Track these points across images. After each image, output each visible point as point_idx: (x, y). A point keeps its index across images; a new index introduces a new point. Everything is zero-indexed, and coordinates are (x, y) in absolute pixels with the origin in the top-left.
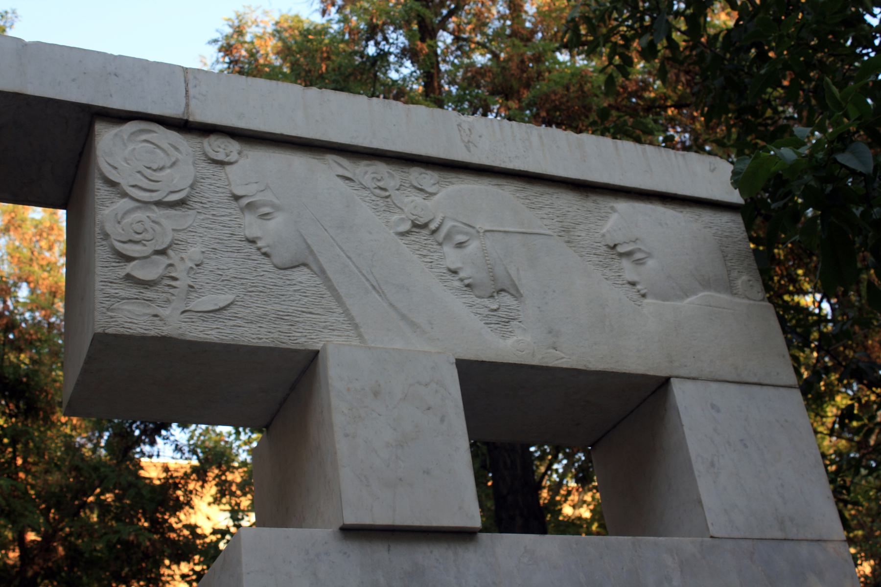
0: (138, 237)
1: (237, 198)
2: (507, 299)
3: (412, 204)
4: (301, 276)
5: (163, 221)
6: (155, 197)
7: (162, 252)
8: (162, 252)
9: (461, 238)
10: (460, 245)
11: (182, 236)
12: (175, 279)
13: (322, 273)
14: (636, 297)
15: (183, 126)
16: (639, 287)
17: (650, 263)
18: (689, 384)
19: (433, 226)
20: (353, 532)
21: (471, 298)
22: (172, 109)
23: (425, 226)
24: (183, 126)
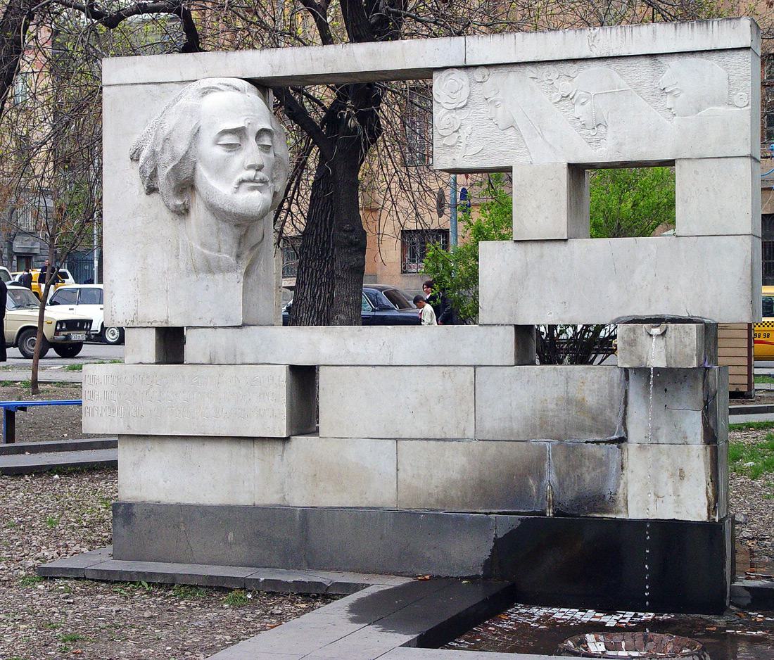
0: (447, 126)
1: (487, 99)
2: (602, 129)
3: (564, 86)
4: (510, 132)
5: (457, 117)
6: (454, 106)
7: (457, 131)
8: (457, 131)
9: (583, 100)
10: (583, 104)
11: (463, 122)
12: (461, 142)
13: (517, 130)
14: (670, 116)
15: (466, 67)
16: (673, 110)
17: (681, 95)
18: (685, 162)
19: (571, 96)
20: (515, 241)
21: (584, 131)
22: (461, 64)
23: (568, 96)
24: (466, 67)
